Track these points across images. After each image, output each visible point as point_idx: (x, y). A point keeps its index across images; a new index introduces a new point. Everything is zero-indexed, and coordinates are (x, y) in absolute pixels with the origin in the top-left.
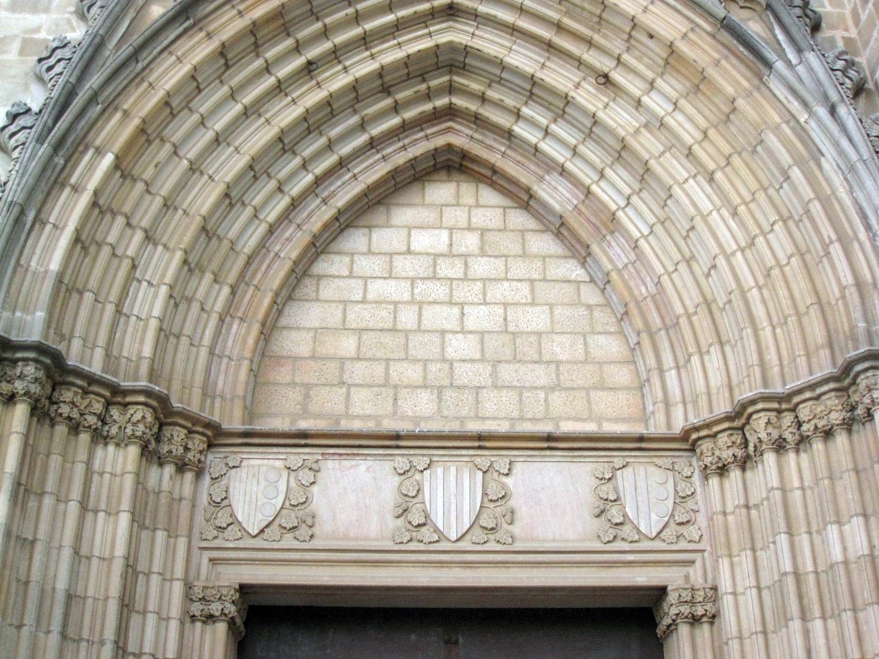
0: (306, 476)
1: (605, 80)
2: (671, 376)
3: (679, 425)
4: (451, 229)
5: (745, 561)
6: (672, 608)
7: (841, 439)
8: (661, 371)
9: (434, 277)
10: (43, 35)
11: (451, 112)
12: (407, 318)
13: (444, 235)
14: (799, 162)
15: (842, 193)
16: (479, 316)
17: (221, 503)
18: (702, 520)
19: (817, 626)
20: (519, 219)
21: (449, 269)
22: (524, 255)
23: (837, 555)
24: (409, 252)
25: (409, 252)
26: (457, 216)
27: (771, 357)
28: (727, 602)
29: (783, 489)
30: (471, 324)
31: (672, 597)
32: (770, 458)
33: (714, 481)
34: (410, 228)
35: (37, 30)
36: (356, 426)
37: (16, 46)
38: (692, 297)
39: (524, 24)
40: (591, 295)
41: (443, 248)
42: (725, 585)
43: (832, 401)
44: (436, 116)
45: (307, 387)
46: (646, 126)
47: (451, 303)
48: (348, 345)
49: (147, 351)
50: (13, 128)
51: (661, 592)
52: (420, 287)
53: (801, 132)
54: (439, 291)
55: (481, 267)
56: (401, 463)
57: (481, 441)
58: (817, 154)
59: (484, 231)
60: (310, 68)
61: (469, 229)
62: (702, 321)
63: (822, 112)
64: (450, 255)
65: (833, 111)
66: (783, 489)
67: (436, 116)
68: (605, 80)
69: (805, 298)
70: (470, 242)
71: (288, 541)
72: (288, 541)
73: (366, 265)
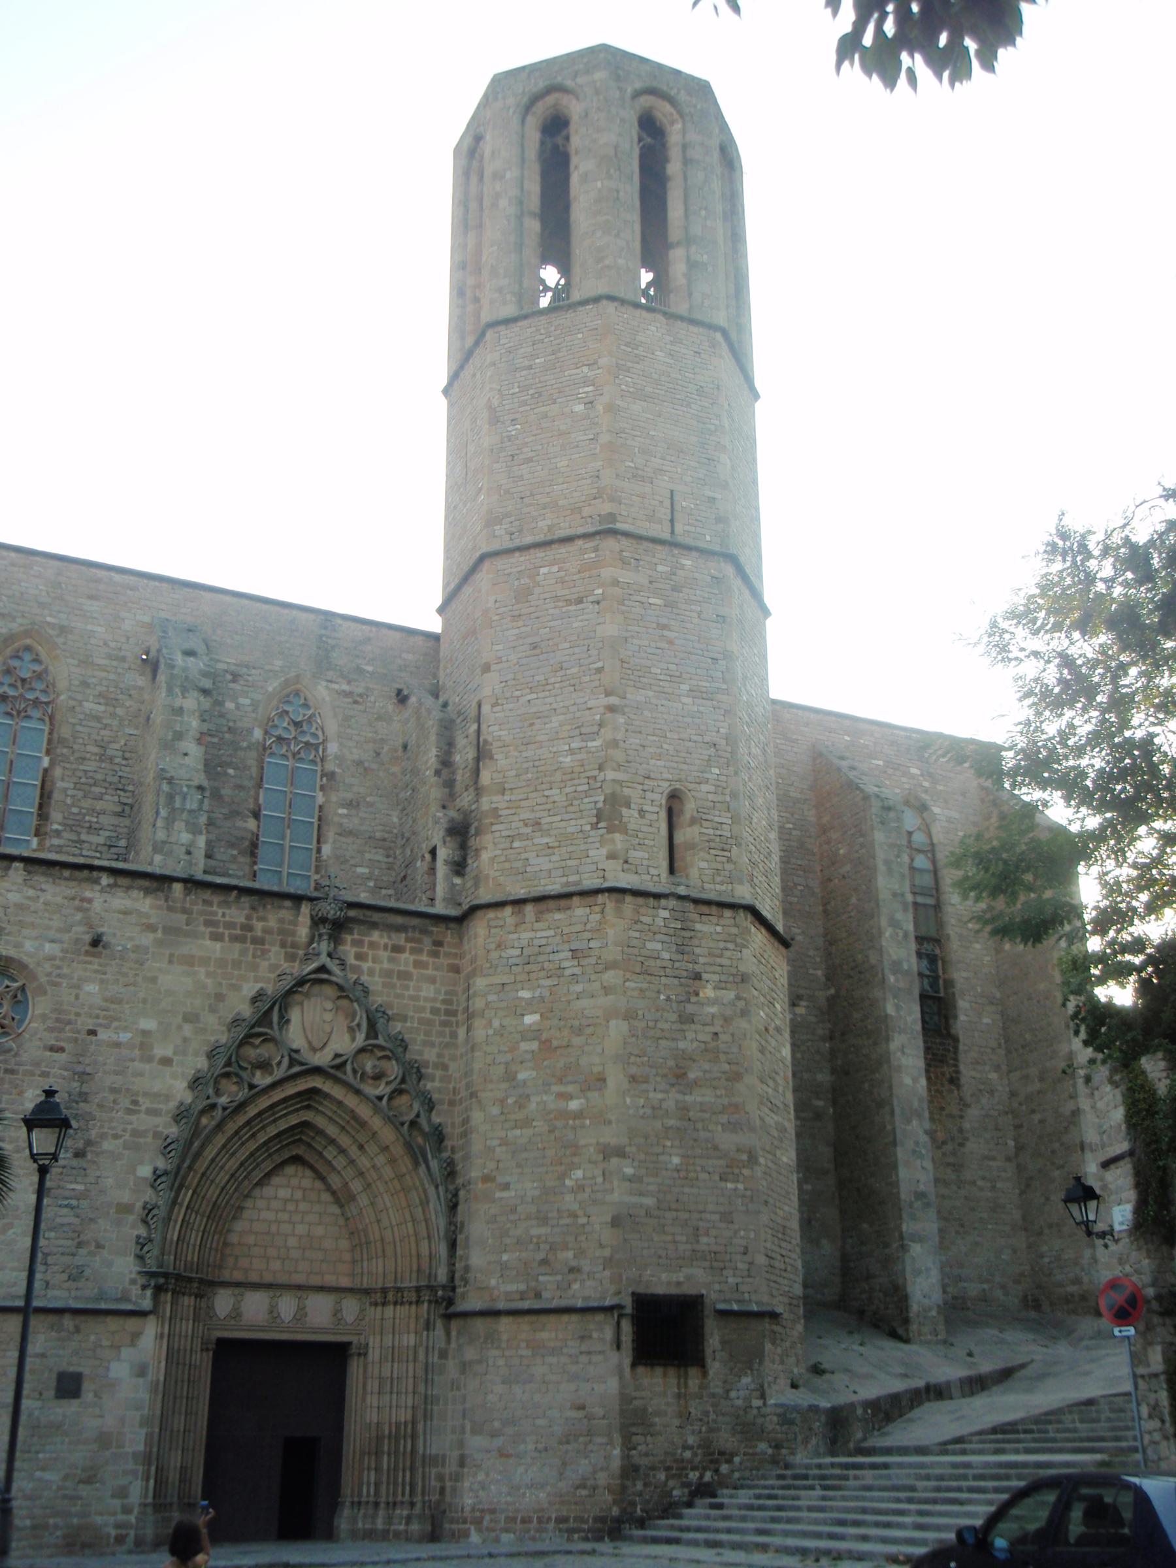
0: (239, 1298)
1: (361, 1147)
2: (365, 1264)
3: (365, 1286)
4: (293, 1188)
5: (378, 1338)
6: (354, 1350)
7: (414, 1307)
8: (362, 1260)
9: (284, 1210)
10: (160, 1129)
11: (300, 1140)
12: (274, 1228)
13: (290, 1191)
14: (421, 1204)
15: (433, 1217)
16: (301, 1229)
17: (211, 1308)
18: (367, 1319)
19: (396, 1365)
20: (318, 1184)
21: (291, 1207)
22: (319, 1202)
23: (405, 1344)
24: (276, 1198)
25: (276, 1198)
26: (295, 1182)
27: (399, 1269)
28: (371, 1351)
29: (394, 1318)
30: (297, 1232)
31: (354, 1346)
32: (392, 1307)
33: (373, 1308)
34: (277, 1186)
35: (158, 1126)
36: (254, 1277)
37: (151, 1135)
38: (377, 1237)
39: (334, 1117)
40: (341, 1221)
41: (289, 1196)
42: (371, 1344)
43: (414, 1294)
44: (294, 1142)
45: (237, 1257)
46: (374, 1167)
47: (290, 1222)
48: (251, 1239)
49: (196, 1259)
50: (159, 1181)
51: (350, 1344)
52: (280, 1214)
53: (425, 1191)
54: (286, 1216)
55: (303, 1206)
56: (271, 1294)
57: (299, 1287)
58: (428, 1202)
59: (305, 1190)
60: (253, 1135)
61: (299, 1188)
62: (379, 1244)
63: (433, 1188)
64: (291, 1200)
65: (437, 1187)
66: (394, 1318)
67: (294, 1142)
69: (414, 1252)
70: (299, 1194)
71: (233, 1322)
72: (233, 1322)
73: (260, 1204)
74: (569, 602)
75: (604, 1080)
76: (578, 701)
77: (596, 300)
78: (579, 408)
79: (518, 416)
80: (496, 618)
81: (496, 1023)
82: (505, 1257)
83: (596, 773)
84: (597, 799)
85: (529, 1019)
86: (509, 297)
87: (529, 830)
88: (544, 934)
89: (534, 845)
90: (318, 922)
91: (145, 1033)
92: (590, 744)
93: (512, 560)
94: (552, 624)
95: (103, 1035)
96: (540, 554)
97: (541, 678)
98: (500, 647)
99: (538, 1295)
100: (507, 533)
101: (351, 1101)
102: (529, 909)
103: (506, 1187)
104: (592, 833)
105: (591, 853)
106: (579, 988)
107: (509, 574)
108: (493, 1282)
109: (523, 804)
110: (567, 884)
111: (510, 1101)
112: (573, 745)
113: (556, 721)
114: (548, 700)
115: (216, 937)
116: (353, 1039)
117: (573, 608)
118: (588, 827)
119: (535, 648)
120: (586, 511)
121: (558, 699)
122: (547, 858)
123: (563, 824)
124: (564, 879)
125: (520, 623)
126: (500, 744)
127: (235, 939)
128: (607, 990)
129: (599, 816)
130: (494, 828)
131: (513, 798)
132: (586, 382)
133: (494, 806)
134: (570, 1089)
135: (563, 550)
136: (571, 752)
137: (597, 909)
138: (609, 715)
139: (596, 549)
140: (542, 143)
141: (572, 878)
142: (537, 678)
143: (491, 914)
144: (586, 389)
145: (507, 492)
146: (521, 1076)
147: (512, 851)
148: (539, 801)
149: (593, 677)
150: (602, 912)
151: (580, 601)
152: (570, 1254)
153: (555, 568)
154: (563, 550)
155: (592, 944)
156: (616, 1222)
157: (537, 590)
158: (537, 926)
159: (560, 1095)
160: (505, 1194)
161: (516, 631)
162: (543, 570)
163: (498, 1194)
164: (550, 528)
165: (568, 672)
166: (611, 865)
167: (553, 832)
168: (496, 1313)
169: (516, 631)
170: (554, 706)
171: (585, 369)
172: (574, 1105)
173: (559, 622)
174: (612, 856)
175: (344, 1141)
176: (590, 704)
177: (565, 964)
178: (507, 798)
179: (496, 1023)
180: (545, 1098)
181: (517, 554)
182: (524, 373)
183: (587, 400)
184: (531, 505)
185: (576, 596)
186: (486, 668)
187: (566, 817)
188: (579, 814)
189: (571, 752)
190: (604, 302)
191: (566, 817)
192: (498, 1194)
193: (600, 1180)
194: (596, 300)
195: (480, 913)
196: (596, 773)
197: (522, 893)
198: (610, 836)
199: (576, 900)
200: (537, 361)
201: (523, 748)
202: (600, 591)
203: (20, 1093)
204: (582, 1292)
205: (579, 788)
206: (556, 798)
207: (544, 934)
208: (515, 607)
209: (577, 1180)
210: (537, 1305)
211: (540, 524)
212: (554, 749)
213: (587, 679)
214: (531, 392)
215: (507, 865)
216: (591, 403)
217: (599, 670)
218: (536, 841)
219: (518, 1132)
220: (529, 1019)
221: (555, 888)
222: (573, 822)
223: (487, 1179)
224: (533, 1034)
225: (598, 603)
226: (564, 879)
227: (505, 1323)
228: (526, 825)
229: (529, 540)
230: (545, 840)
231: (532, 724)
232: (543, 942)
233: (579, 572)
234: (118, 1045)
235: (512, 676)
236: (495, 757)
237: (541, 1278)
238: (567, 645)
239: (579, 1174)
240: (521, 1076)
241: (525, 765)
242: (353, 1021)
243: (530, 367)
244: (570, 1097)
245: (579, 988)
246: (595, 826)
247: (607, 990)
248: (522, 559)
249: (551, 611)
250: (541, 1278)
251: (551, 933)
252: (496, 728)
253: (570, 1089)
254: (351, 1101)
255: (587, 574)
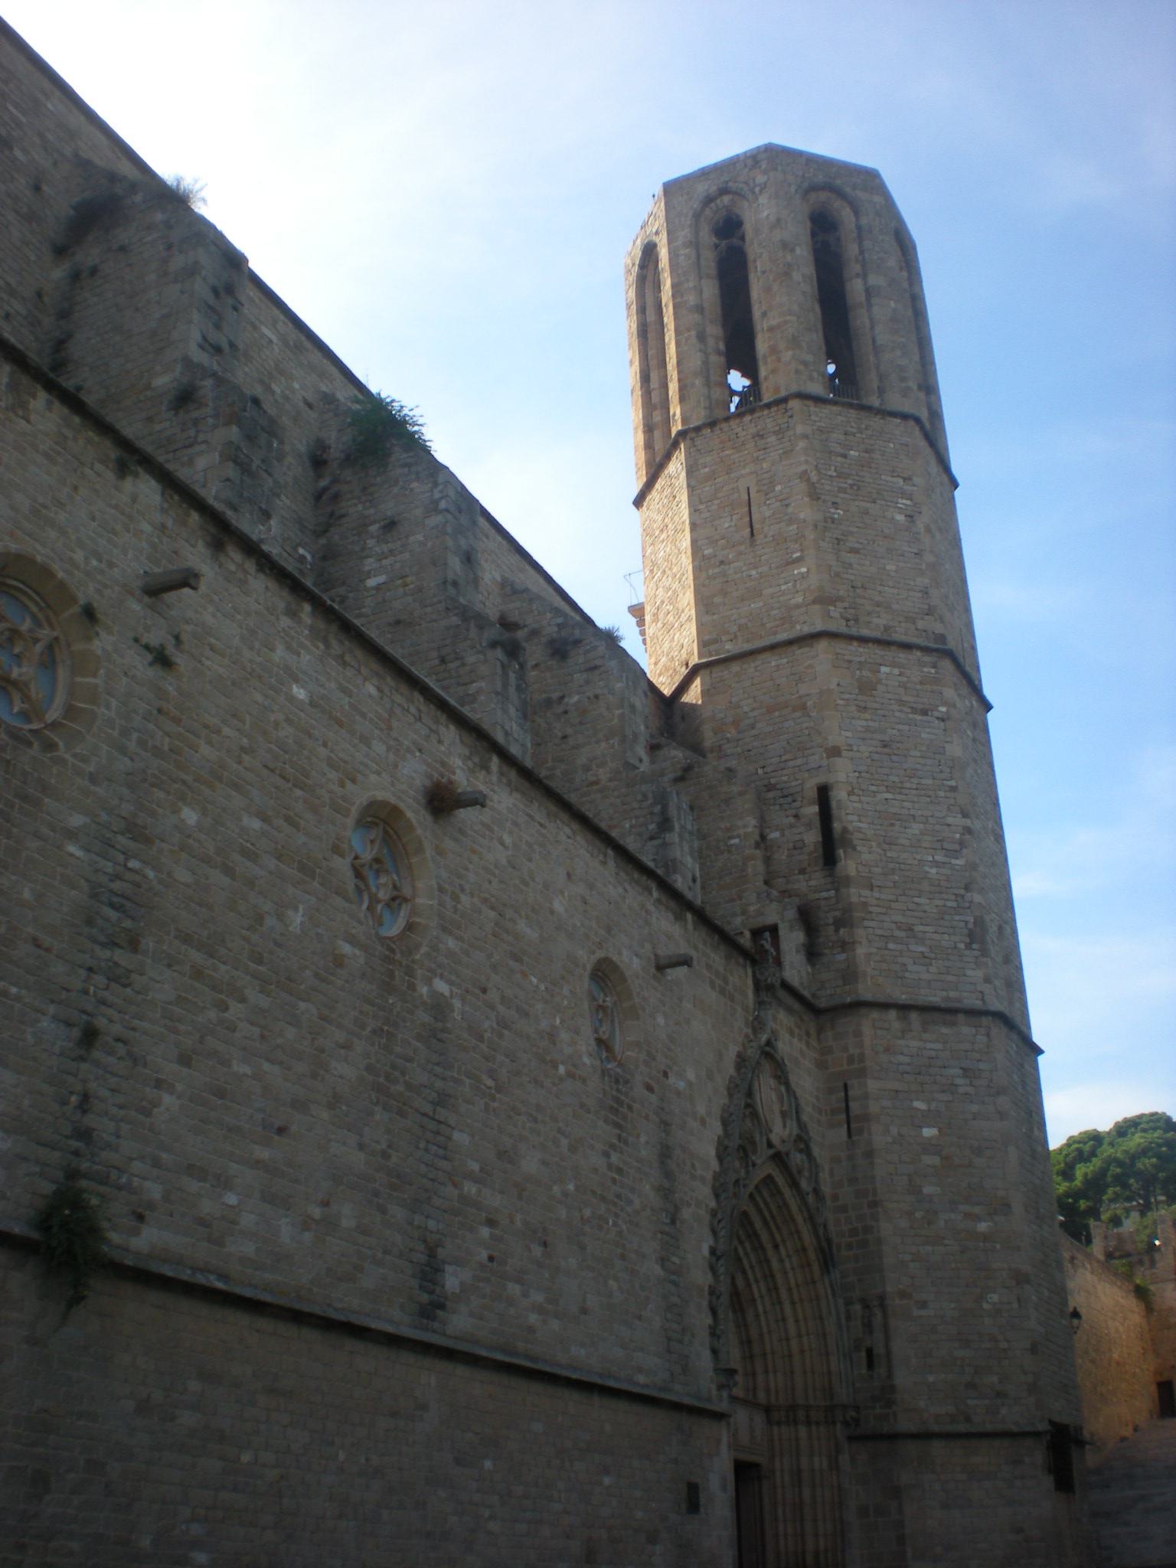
1: (776, 1247)
68: (776, 1247)
74: (914, 711)
75: (1008, 1206)
76: (937, 814)
77: (905, 417)
78: (900, 518)
79: (838, 500)
80: (841, 702)
81: (894, 1130)
82: (931, 1379)
83: (962, 892)
84: (967, 919)
85: (928, 1132)
86: (815, 375)
87: (902, 934)
88: (932, 1046)
89: (909, 950)
90: (758, 987)
91: (690, 1084)
92: (954, 861)
93: (850, 647)
94: (901, 727)
95: (672, 1080)
96: (878, 652)
97: (896, 779)
98: (849, 734)
99: (968, 1419)
100: (842, 617)
101: (787, 1192)
102: (914, 1016)
103: (923, 1305)
104: (967, 952)
105: (969, 972)
106: (975, 1108)
107: (850, 662)
108: (922, 1404)
109: (893, 905)
110: (948, 999)
111: (918, 1215)
112: (937, 858)
113: (916, 828)
114: (905, 804)
115: (712, 985)
116: (785, 1126)
117: (918, 717)
118: (962, 946)
119: (885, 746)
120: (920, 624)
121: (917, 806)
122: (925, 968)
123: (937, 937)
124: (944, 994)
125: (867, 716)
126: (861, 836)
127: (722, 991)
128: (1002, 1115)
129: (971, 935)
130: (866, 923)
131: (883, 896)
132: (904, 495)
133: (863, 899)
134: (977, 1210)
135: (901, 655)
136: (936, 864)
137: (982, 1031)
138: (967, 836)
139: (934, 666)
140: (813, 235)
141: (952, 994)
142: (892, 778)
143: (875, 1014)
144: (904, 501)
145: (837, 575)
146: (927, 1190)
147: (886, 952)
148: (912, 906)
149: (948, 794)
150: (988, 1035)
151: (924, 712)
152: (995, 1379)
153: (896, 671)
154: (902, 656)
155: (982, 1066)
156: (1034, 1349)
157: (881, 688)
158: (926, 1036)
159: (967, 1215)
160: (922, 1313)
161: (864, 723)
162: (883, 669)
163: (916, 1312)
164: (887, 628)
165: (923, 781)
166: (987, 988)
167: (928, 942)
168: (926, 1436)
169: (864, 723)
170: (912, 812)
171: (901, 481)
172: (983, 1227)
173: (907, 727)
174: (987, 980)
175: (764, 1236)
176: (950, 820)
177: (959, 1081)
178: (876, 895)
179: (894, 1130)
180: (953, 1216)
181: (855, 644)
182: (839, 459)
183: (908, 513)
184: (864, 598)
185: (921, 706)
186: (835, 752)
187: (941, 930)
188: (951, 930)
189: (936, 864)
190: (912, 423)
191: (941, 930)
192: (916, 1312)
193: (1016, 1305)
194: (905, 417)
195: (863, 1011)
196: (962, 892)
197: (903, 998)
198: (985, 959)
199: (961, 1017)
200: (852, 452)
201: (886, 847)
202: (943, 709)
203: (638, 1136)
204: (1011, 1416)
205: (949, 904)
206: (927, 908)
207: (932, 1046)
208: (860, 697)
209: (995, 1304)
210: (962, 1427)
211: (876, 620)
212: (918, 857)
213: (941, 794)
214: (850, 482)
215: (884, 966)
216: (911, 517)
217: (954, 789)
218: (912, 947)
219: (929, 1248)
220: (928, 1132)
221: (936, 998)
222: (946, 937)
223: (903, 1295)
224: (929, 1147)
225: (943, 720)
226: (944, 994)
227: (937, 1448)
228: (899, 928)
229: (865, 632)
230: (921, 949)
231: (892, 825)
232: (933, 1054)
233: (921, 683)
234: (678, 1093)
235: (865, 768)
236: (858, 848)
237: (969, 1402)
238: (918, 754)
239: (995, 1298)
240: (927, 1190)
241: (891, 865)
242: (782, 1106)
243: (845, 456)
244: (978, 1218)
245: (975, 1108)
246: (968, 946)
247: (1002, 1115)
248: (861, 650)
249: (897, 714)
250: (969, 1402)
251: (939, 1046)
252: (855, 818)
253: (977, 1210)
254: (787, 1192)
255: (928, 687)
